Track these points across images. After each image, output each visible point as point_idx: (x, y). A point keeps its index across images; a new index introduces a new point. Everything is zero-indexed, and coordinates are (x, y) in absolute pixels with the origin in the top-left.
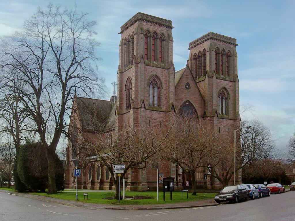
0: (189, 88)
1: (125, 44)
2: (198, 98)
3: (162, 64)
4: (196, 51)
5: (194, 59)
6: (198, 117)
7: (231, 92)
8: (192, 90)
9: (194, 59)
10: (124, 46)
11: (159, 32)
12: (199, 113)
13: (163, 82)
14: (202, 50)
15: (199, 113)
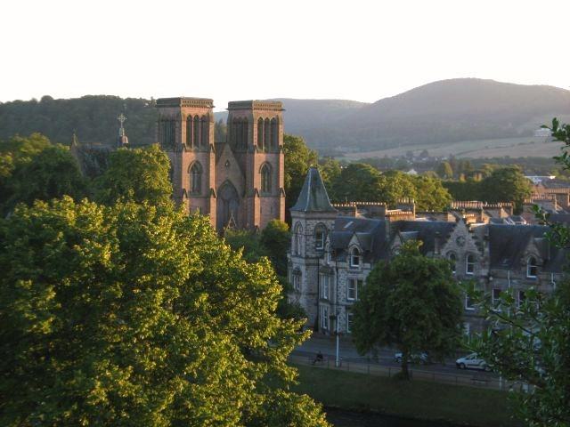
0: (229, 165)
1: (162, 121)
2: (239, 174)
3: (203, 148)
4: (237, 115)
5: (234, 123)
6: (237, 196)
7: (274, 165)
8: (231, 167)
9: (234, 123)
10: (161, 123)
11: (200, 115)
12: (239, 192)
13: (204, 167)
14: (243, 117)
15: (239, 192)
